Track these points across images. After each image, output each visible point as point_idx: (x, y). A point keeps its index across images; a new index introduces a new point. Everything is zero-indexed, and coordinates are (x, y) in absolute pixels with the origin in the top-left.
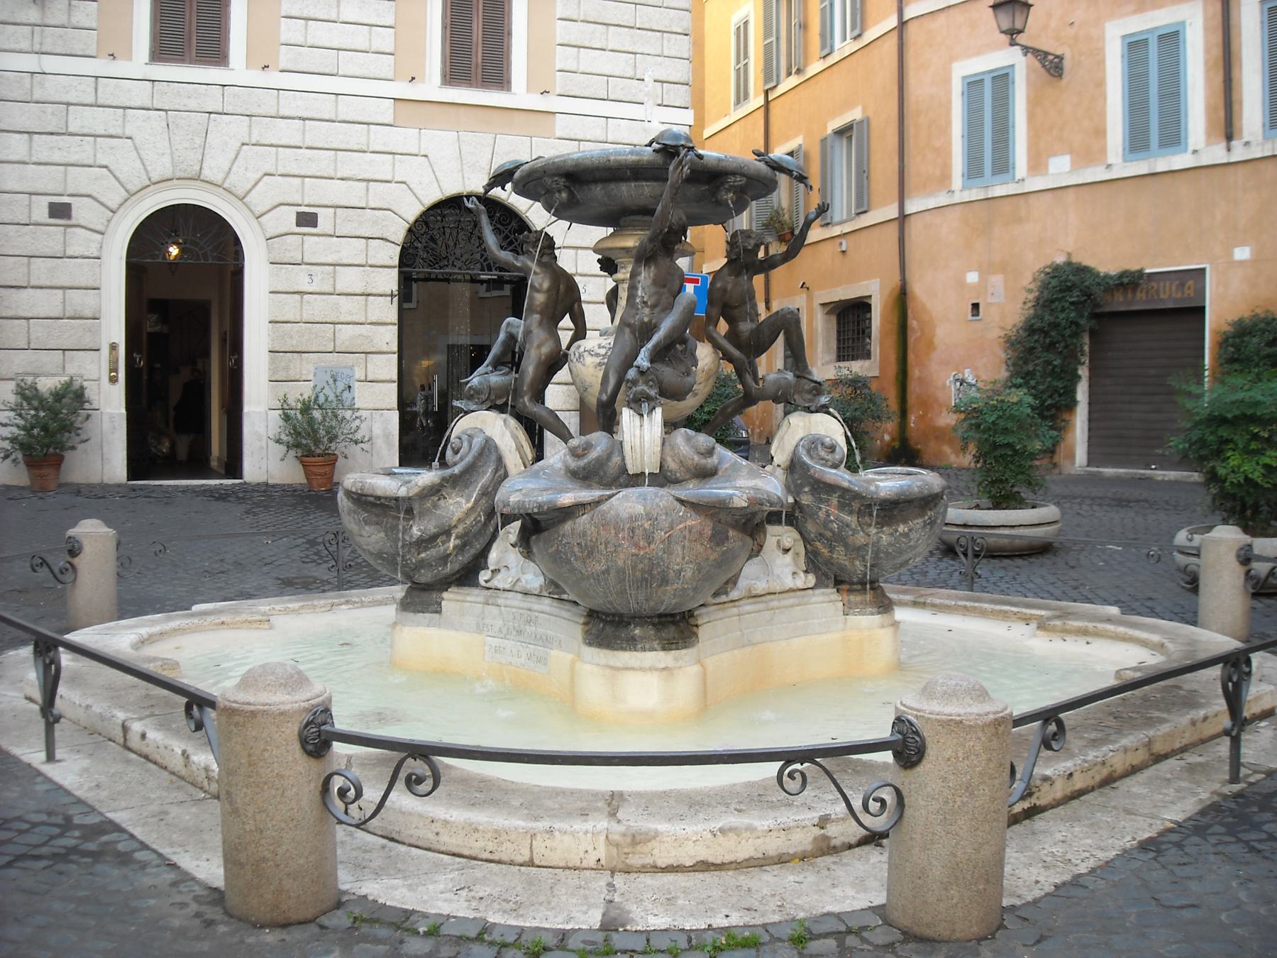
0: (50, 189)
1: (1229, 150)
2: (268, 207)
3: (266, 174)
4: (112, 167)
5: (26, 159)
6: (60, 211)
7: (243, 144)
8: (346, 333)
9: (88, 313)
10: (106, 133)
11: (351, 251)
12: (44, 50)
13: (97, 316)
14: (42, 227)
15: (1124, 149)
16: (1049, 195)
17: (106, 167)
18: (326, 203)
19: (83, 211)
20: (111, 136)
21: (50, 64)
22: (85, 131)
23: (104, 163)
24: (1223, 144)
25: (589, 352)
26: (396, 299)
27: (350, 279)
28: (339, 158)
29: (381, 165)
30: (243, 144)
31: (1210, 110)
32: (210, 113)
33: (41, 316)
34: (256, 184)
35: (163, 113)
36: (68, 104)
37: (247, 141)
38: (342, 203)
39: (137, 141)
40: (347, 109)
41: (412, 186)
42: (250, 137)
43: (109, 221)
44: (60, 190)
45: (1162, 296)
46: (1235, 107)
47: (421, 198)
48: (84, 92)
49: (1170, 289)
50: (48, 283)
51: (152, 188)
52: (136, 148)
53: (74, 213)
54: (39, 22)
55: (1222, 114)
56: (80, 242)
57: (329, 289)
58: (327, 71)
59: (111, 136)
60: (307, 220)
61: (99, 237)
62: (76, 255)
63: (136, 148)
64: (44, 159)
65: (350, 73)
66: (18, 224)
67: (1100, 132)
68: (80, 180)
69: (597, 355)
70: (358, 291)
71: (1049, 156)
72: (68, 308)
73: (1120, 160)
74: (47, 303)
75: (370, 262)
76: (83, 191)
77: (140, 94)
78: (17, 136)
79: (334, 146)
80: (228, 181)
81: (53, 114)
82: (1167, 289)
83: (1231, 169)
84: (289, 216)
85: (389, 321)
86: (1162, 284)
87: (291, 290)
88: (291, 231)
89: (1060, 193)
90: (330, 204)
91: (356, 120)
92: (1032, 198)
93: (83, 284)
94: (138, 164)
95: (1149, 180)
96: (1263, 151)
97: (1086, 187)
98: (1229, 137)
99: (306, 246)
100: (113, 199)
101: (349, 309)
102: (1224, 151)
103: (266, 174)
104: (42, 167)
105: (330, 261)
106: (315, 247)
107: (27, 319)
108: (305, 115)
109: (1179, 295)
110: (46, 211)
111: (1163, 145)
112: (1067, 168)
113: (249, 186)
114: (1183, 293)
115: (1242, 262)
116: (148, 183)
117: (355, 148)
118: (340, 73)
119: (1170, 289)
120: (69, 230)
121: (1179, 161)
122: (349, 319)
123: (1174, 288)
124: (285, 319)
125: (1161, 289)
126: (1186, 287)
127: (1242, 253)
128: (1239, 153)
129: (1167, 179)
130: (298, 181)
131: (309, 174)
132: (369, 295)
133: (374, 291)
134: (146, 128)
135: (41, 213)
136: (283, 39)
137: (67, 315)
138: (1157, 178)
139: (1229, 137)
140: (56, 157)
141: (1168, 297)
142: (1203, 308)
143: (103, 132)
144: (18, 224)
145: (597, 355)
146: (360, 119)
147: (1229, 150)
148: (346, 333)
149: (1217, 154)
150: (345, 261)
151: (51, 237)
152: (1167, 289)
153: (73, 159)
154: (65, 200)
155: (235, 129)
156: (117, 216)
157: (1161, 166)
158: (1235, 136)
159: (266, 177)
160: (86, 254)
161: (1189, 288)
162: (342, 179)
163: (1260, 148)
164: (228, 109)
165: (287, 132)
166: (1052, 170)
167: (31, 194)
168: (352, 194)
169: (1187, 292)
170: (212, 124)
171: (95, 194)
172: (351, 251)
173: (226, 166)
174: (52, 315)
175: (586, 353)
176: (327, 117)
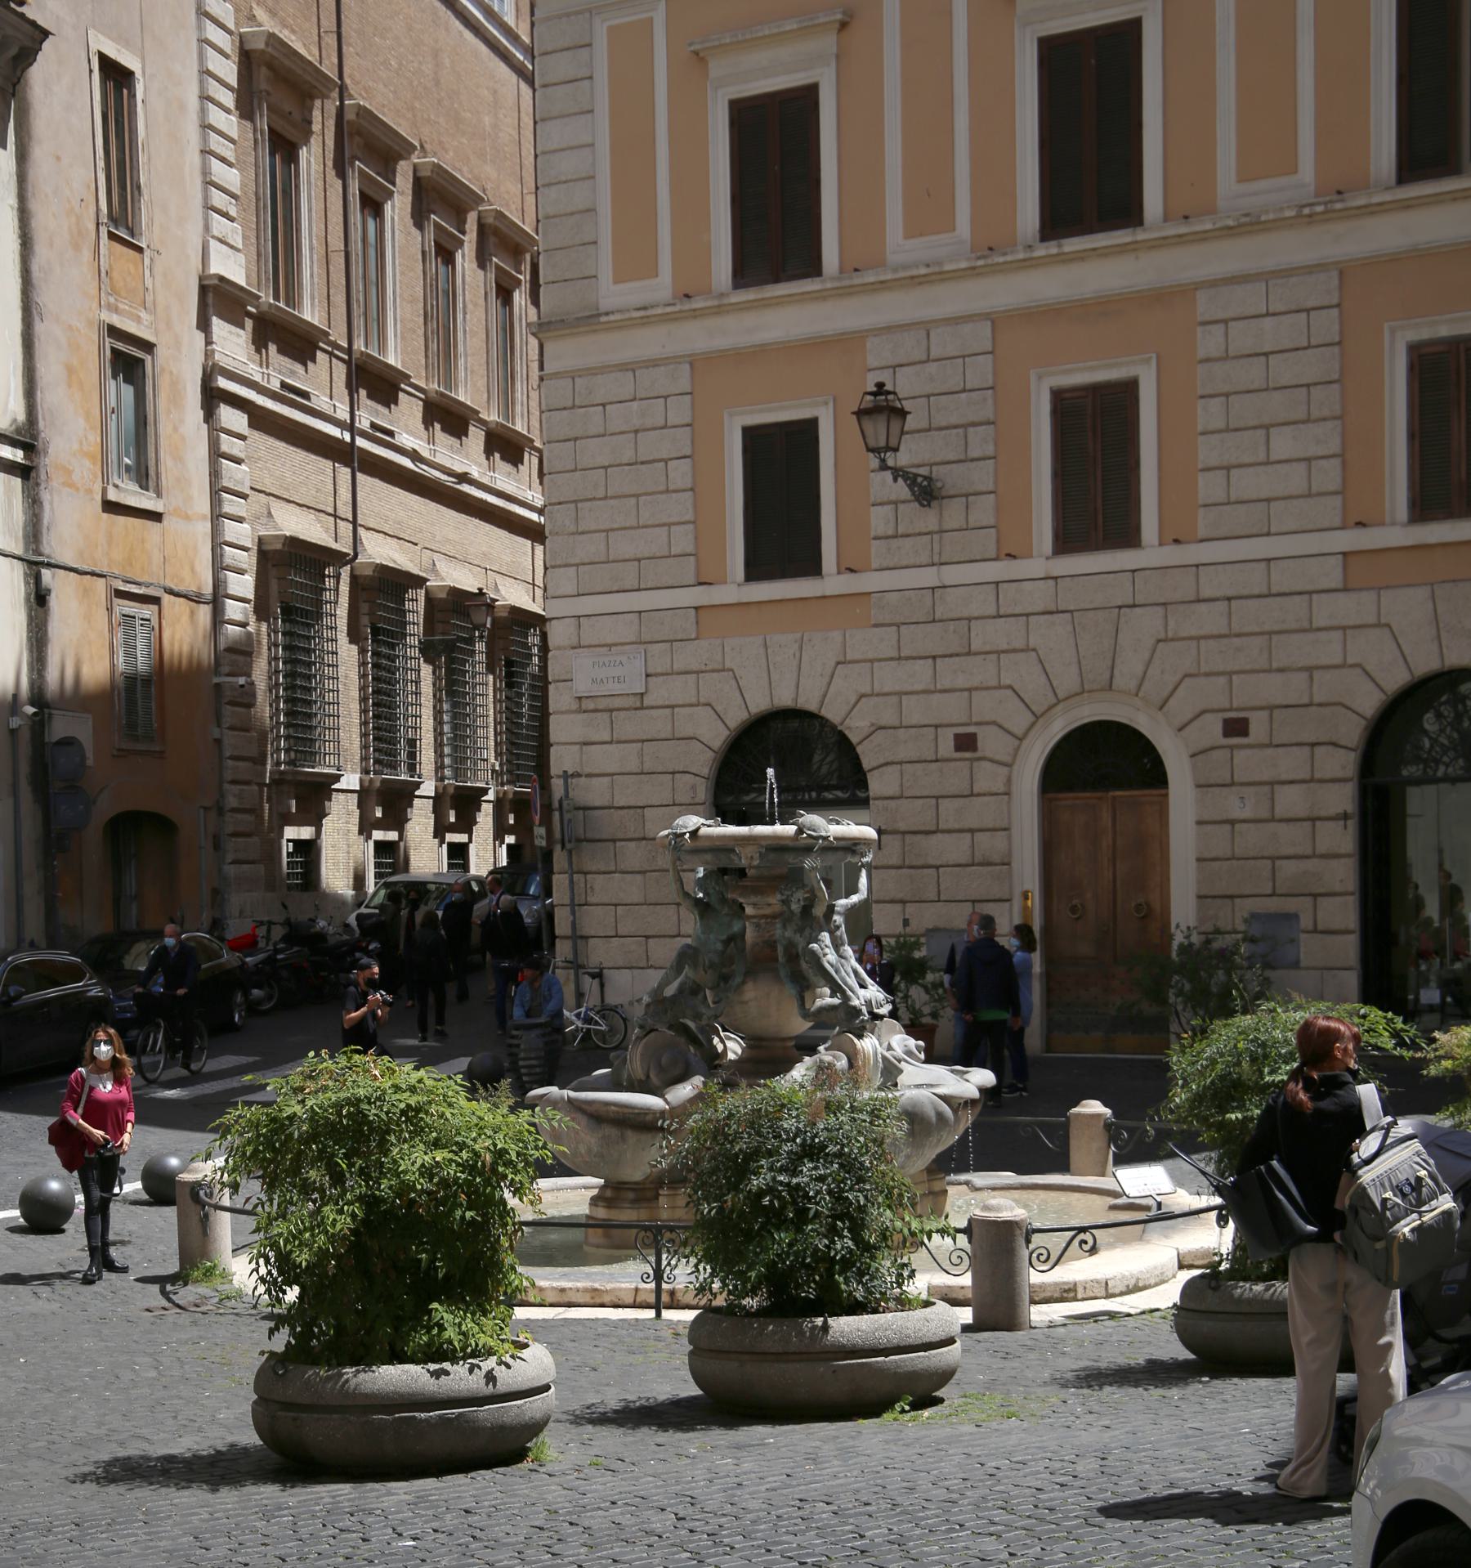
0: (955, 720)
2: (1190, 716)
3: (1186, 676)
4: (1015, 687)
5: (932, 687)
6: (966, 743)
7: (1159, 641)
8: (1288, 868)
9: (996, 858)
10: (1010, 647)
11: (1291, 763)
12: (943, 561)
13: (1006, 861)
14: (952, 764)
17: (1010, 687)
18: (1258, 703)
19: (991, 743)
20: (1014, 651)
21: (952, 574)
22: (988, 648)
23: (1008, 682)
26: (1352, 825)
27: (1290, 800)
28: (1273, 644)
29: (1329, 649)
30: (1159, 641)
32: (1120, 607)
33: (951, 863)
34: (1176, 688)
35: (1068, 615)
36: (969, 619)
37: (1162, 636)
38: (1278, 702)
39: (1040, 652)
40: (1282, 578)
41: (1368, 668)
42: (1166, 632)
43: (1017, 750)
44: (964, 719)
47: (1382, 683)
48: (982, 604)
50: (957, 826)
51: (1060, 707)
52: (1041, 661)
53: (979, 744)
54: (936, 528)
56: (988, 778)
57: (1265, 815)
58: (1254, 531)
59: (1014, 651)
60: (1236, 727)
61: (1005, 770)
62: (981, 791)
63: (1041, 661)
64: (947, 685)
65: (1284, 529)
66: (925, 761)
68: (985, 707)
70: (1302, 815)
72: (977, 853)
74: (953, 849)
75: (1317, 775)
76: (987, 718)
77: (1038, 597)
78: (921, 662)
79: (1267, 628)
80: (1143, 689)
81: (954, 632)
84: (1213, 727)
85: (1343, 851)
87: (1219, 818)
88: (1217, 744)
90: (1264, 703)
91: (1294, 589)
93: (991, 826)
94: (1043, 678)
99: (1235, 761)
100: (1019, 720)
101: (1291, 838)
103: (1186, 676)
104: (946, 695)
105: (1265, 778)
106: (1249, 762)
107: (937, 867)
108: (1230, 593)
110: (952, 743)
113: (1166, 694)
116: (1055, 701)
117: (1294, 626)
118: (1273, 530)
120: (975, 764)
122: (1291, 851)
124: (1213, 855)
130: (1222, 680)
131: (1237, 668)
132: (1320, 819)
133: (1323, 813)
134: (1051, 636)
135: (947, 746)
136: (1202, 497)
137: (976, 861)
140: (961, 682)
143: (1005, 647)
144: (925, 761)
146: (1299, 588)
148: (1288, 868)
150: (1284, 777)
151: (954, 777)
153: (975, 683)
154: (971, 729)
155: (1147, 623)
156: (1025, 743)
159: (1186, 679)
160: (994, 790)
162: (1281, 670)
164: (1140, 600)
165: (1210, 619)
167: (936, 727)
168: (1293, 688)
170: (1122, 620)
171: (999, 721)
172: (1291, 763)
173: (1140, 669)
174: (963, 862)
176: (1256, 591)
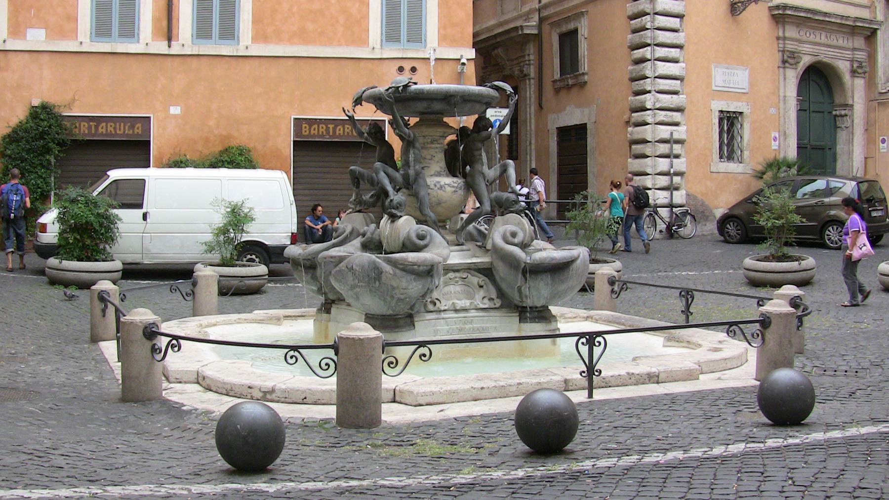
1: (169, 46)
15: (91, 33)
16: (27, 55)
24: (167, 42)
25: (449, 185)
31: (156, 20)
45: (118, 132)
46: (174, 21)
49: (124, 128)
55: (165, 23)
67: (73, 19)
69: (453, 187)
71: (27, 27)
73: (88, 40)
82: (122, 128)
83: (169, 59)
86: (118, 124)
89: (35, 54)
92: (11, 55)
95: (110, 56)
96: (192, 50)
97: (58, 54)
98: (169, 40)
102: (167, 47)
109: (131, 132)
111: (120, 36)
112: (43, 38)
114: (133, 131)
115: (175, 116)
119: (124, 128)
121: (133, 48)
123: (127, 127)
125: (118, 127)
126: (136, 128)
127: (175, 110)
128: (176, 49)
129: (124, 58)
138: (114, 56)
139: (169, 40)
141: (122, 132)
142: (149, 141)
145: (453, 187)
147: (169, 46)
149: (161, 47)
152: (122, 128)
157: (121, 48)
158: (173, 39)
161: (138, 129)
163: (190, 49)
166: (29, 37)
169: (136, 131)
175: (446, 186)
